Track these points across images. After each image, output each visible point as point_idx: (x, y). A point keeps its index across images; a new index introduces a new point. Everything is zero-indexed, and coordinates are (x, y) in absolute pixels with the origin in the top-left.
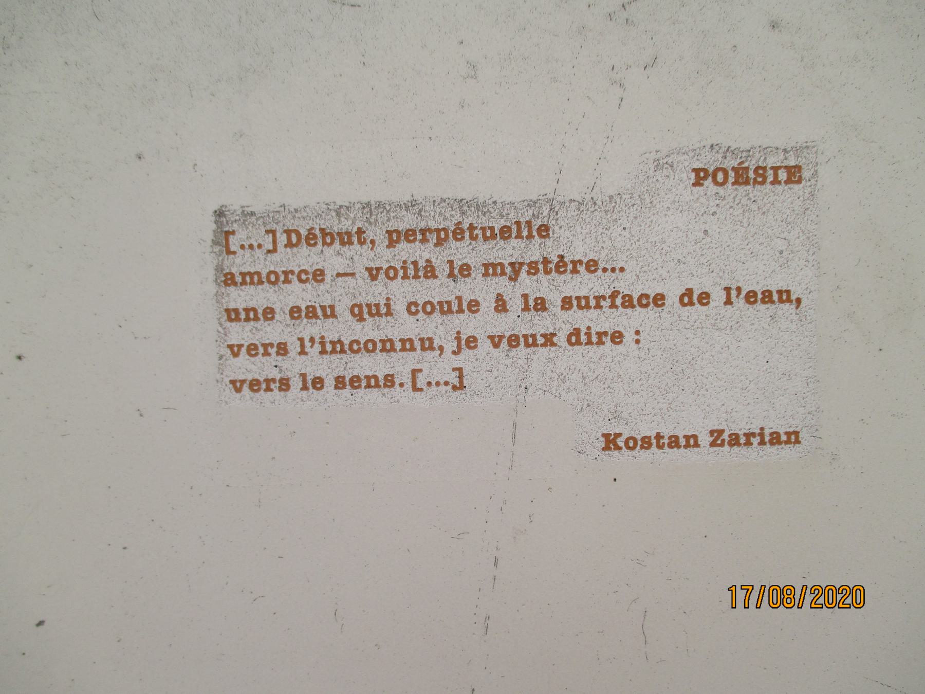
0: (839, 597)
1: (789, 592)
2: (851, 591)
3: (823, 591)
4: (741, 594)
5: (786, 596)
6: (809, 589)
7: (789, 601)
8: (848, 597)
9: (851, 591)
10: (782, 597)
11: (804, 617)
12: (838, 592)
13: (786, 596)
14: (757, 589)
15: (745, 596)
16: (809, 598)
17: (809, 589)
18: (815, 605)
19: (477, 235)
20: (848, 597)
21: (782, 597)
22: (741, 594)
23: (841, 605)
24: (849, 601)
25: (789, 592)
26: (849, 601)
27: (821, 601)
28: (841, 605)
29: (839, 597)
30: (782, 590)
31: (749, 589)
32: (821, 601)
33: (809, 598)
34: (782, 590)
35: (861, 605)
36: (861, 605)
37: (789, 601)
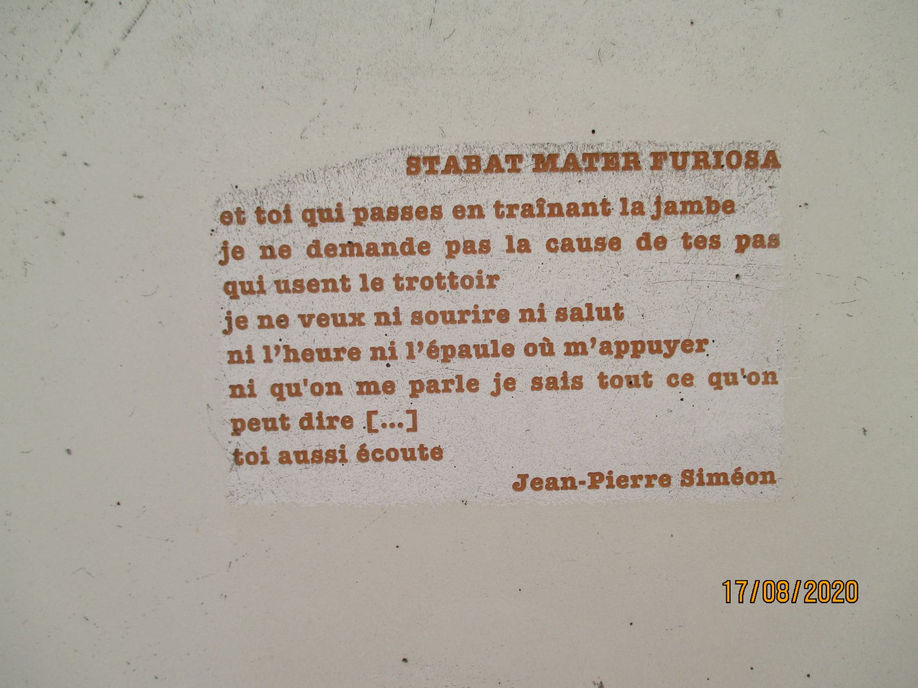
0: (833, 591)
1: (783, 587)
2: (845, 586)
3: (817, 586)
4: (735, 589)
5: (780, 591)
6: (802, 584)
7: (783, 595)
8: (842, 592)
9: (845, 586)
10: (776, 592)
11: (800, 611)
12: (831, 587)
13: (780, 591)
14: (751, 584)
15: (738, 590)
16: (803, 592)
17: (802, 584)
18: (808, 600)
20: (842, 592)
21: (776, 592)
22: (735, 589)
23: (834, 600)
24: (842, 596)
25: (783, 587)
26: (842, 596)
27: (815, 596)
28: (834, 600)
29: (833, 591)
30: (776, 585)
31: (743, 584)
32: (815, 596)
33: (803, 592)
34: (776, 585)
35: (854, 600)
37: (783, 595)
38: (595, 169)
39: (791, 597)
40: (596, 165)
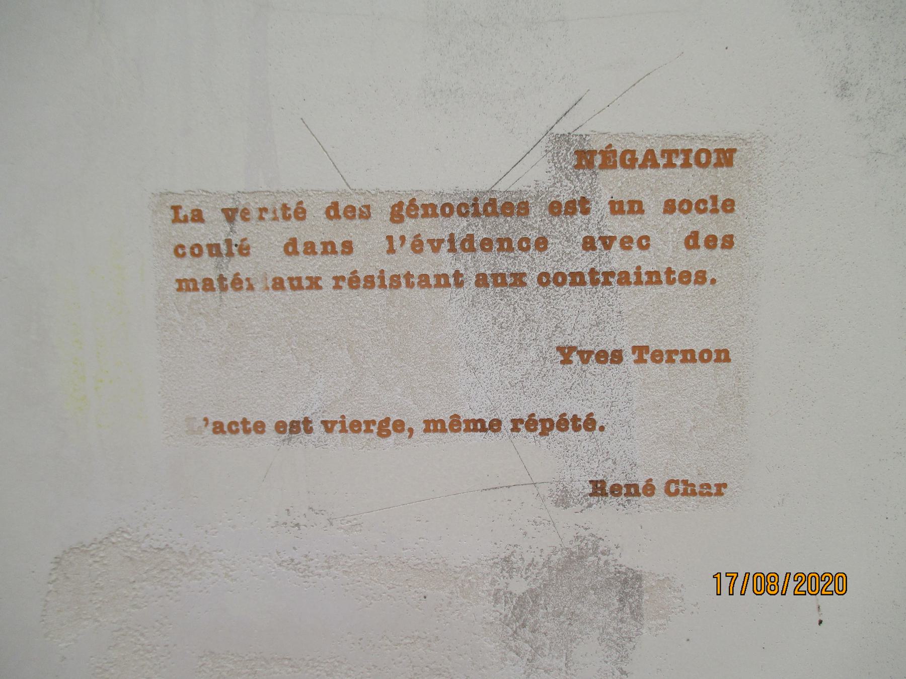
0: (822, 584)
1: (773, 579)
2: (834, 578)
3: (807, 578)
4: (726, 581)
5: (770, 584)
6: (792, 576)
7: (773, 588)
8: (831, 584)
10: (766, 584)
12: (820, 579)
13: (770, 584)
15: (728, 583)
16: (792, 584)
17: (792, 576)
18: (798, 592)
19: (663, 156)
20: (831, 584)
21: (766, 584)
22: (726, 581)
23: (824, 592)
25: (773, 579)
26: (831, 588)
27: (804, 588)
28: (824, 592)
29: (822, 584)
30: (766, 578)
31: (733, 577)
32: (804, 588)
33: (792, 584)
35: (843, 592)
36: (843, 592)
37: (773, 588)
38: (674, 166)
39: (780, 589)
40: (674, 161)
